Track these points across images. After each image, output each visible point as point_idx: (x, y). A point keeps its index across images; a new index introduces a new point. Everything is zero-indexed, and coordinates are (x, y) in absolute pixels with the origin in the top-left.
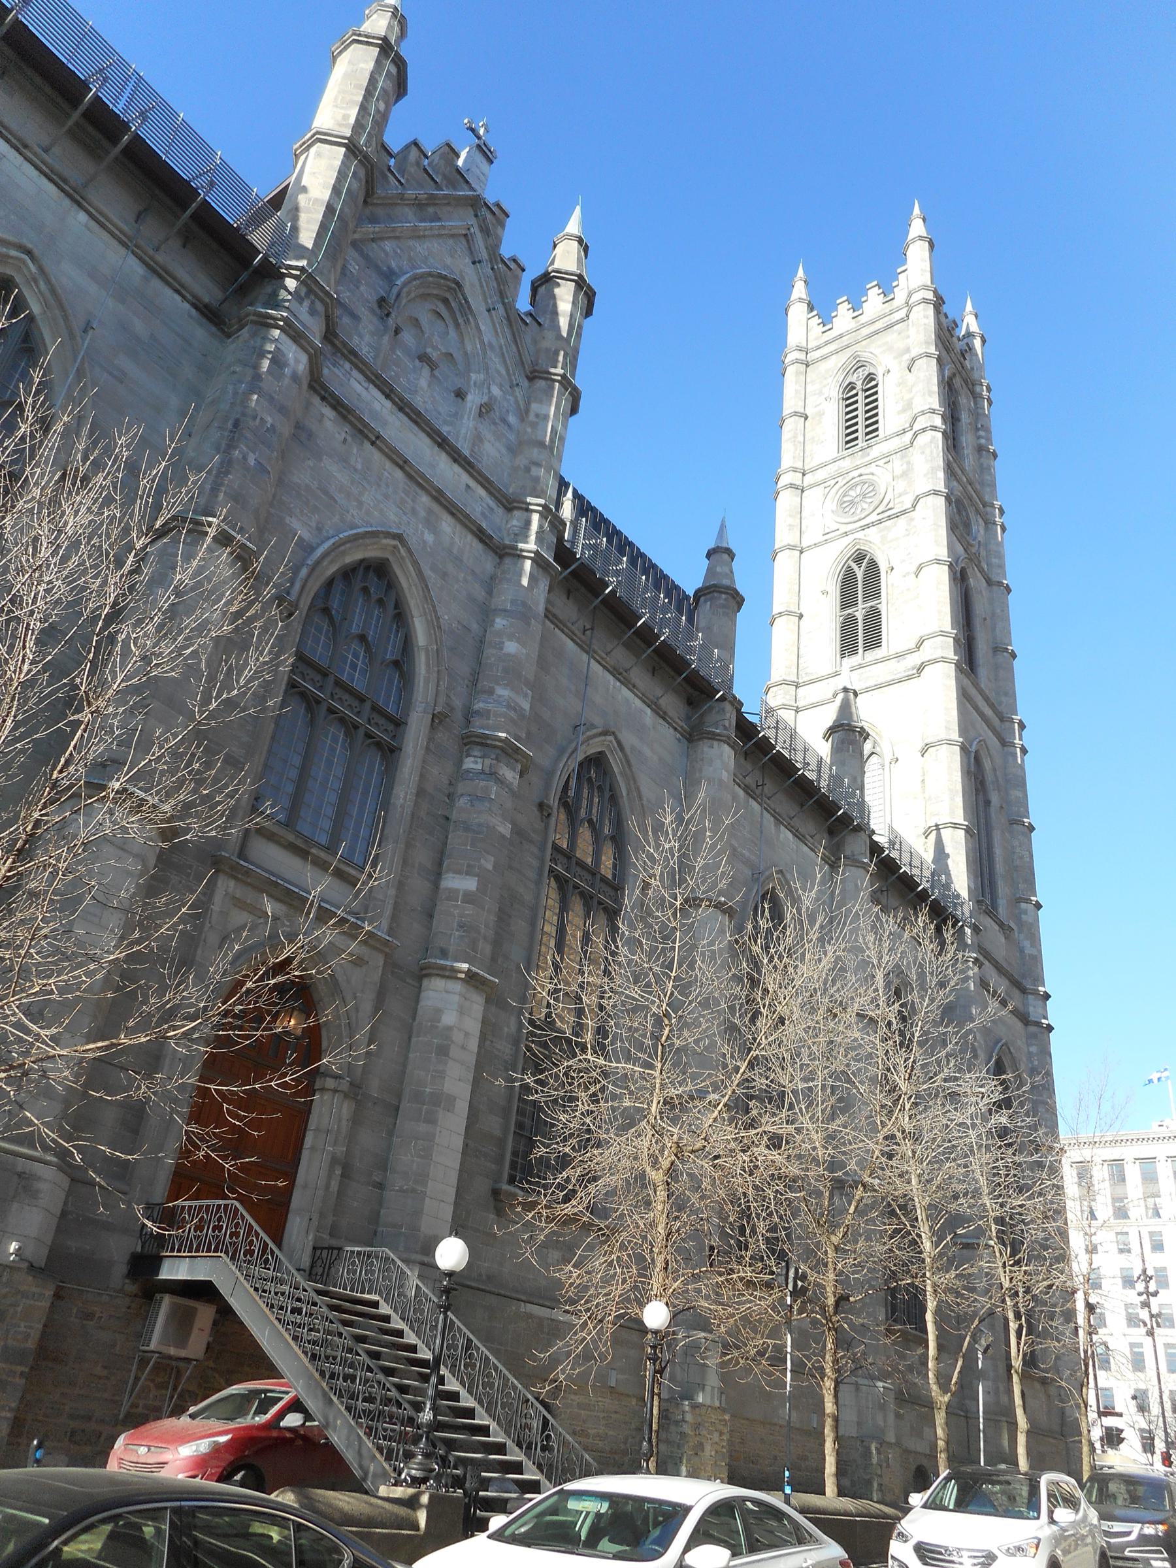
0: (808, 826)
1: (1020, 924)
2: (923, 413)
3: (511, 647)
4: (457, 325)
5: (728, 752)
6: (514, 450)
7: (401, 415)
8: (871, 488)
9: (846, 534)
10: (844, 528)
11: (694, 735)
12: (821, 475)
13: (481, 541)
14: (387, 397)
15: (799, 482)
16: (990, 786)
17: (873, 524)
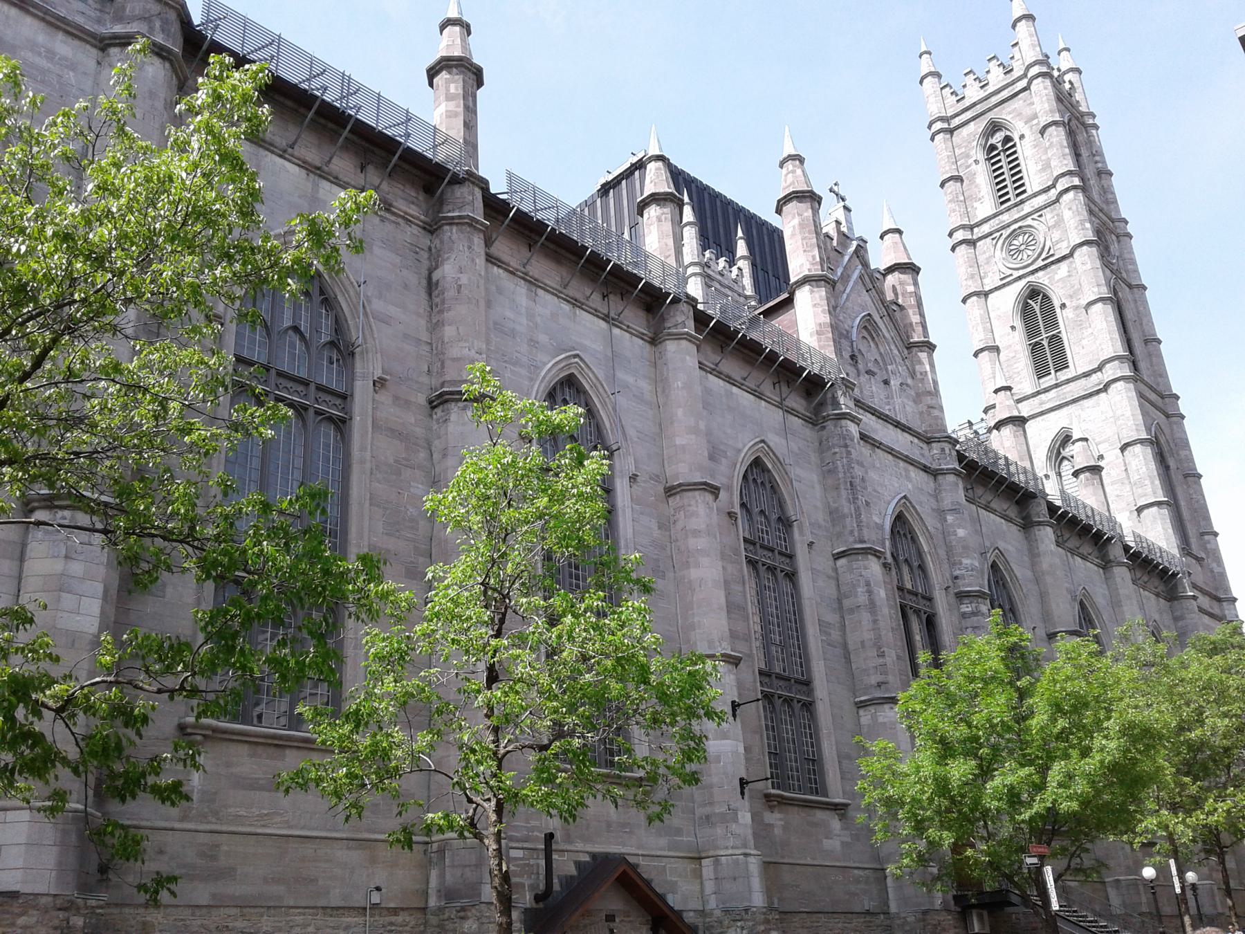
0: (1087, 549)
1: (1206, 550)
2: (1063, 175)
3: (961, 533)
4: (873, 339)
5: (1049, 530)
6: (917, 398)
7: (880, 421)
8: (1031, 238)
9: (1020, 278)
10: (1016, 274)
11: (1027, 525)
12: (986, 228)
13: (926, 471)
14: (873, 414)
15: (970, 237)
16: (1167, 455)
17: (1040, 269)
